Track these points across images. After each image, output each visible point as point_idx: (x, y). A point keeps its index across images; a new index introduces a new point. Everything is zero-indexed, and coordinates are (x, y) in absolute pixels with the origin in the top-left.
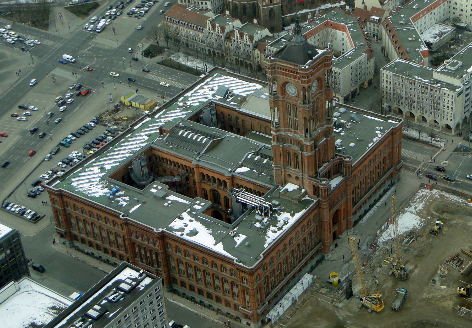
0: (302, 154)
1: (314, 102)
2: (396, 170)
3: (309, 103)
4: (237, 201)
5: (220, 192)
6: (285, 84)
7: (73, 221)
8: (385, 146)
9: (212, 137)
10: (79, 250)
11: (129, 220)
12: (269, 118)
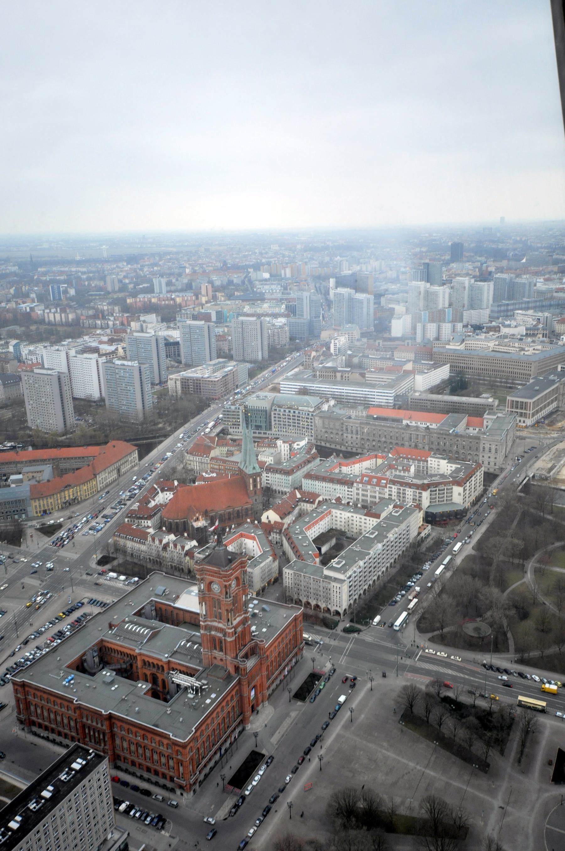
0: (225, 639)
1: (233, 597)
2: (299, 649)
4: (173, 682)
5: (158, 675)
6: (210, 583)
7: (32, 708)
8: (290, 630)
9: (152, 628)
10: (35, 734)
11: (81, 704)
12: (198, 611)
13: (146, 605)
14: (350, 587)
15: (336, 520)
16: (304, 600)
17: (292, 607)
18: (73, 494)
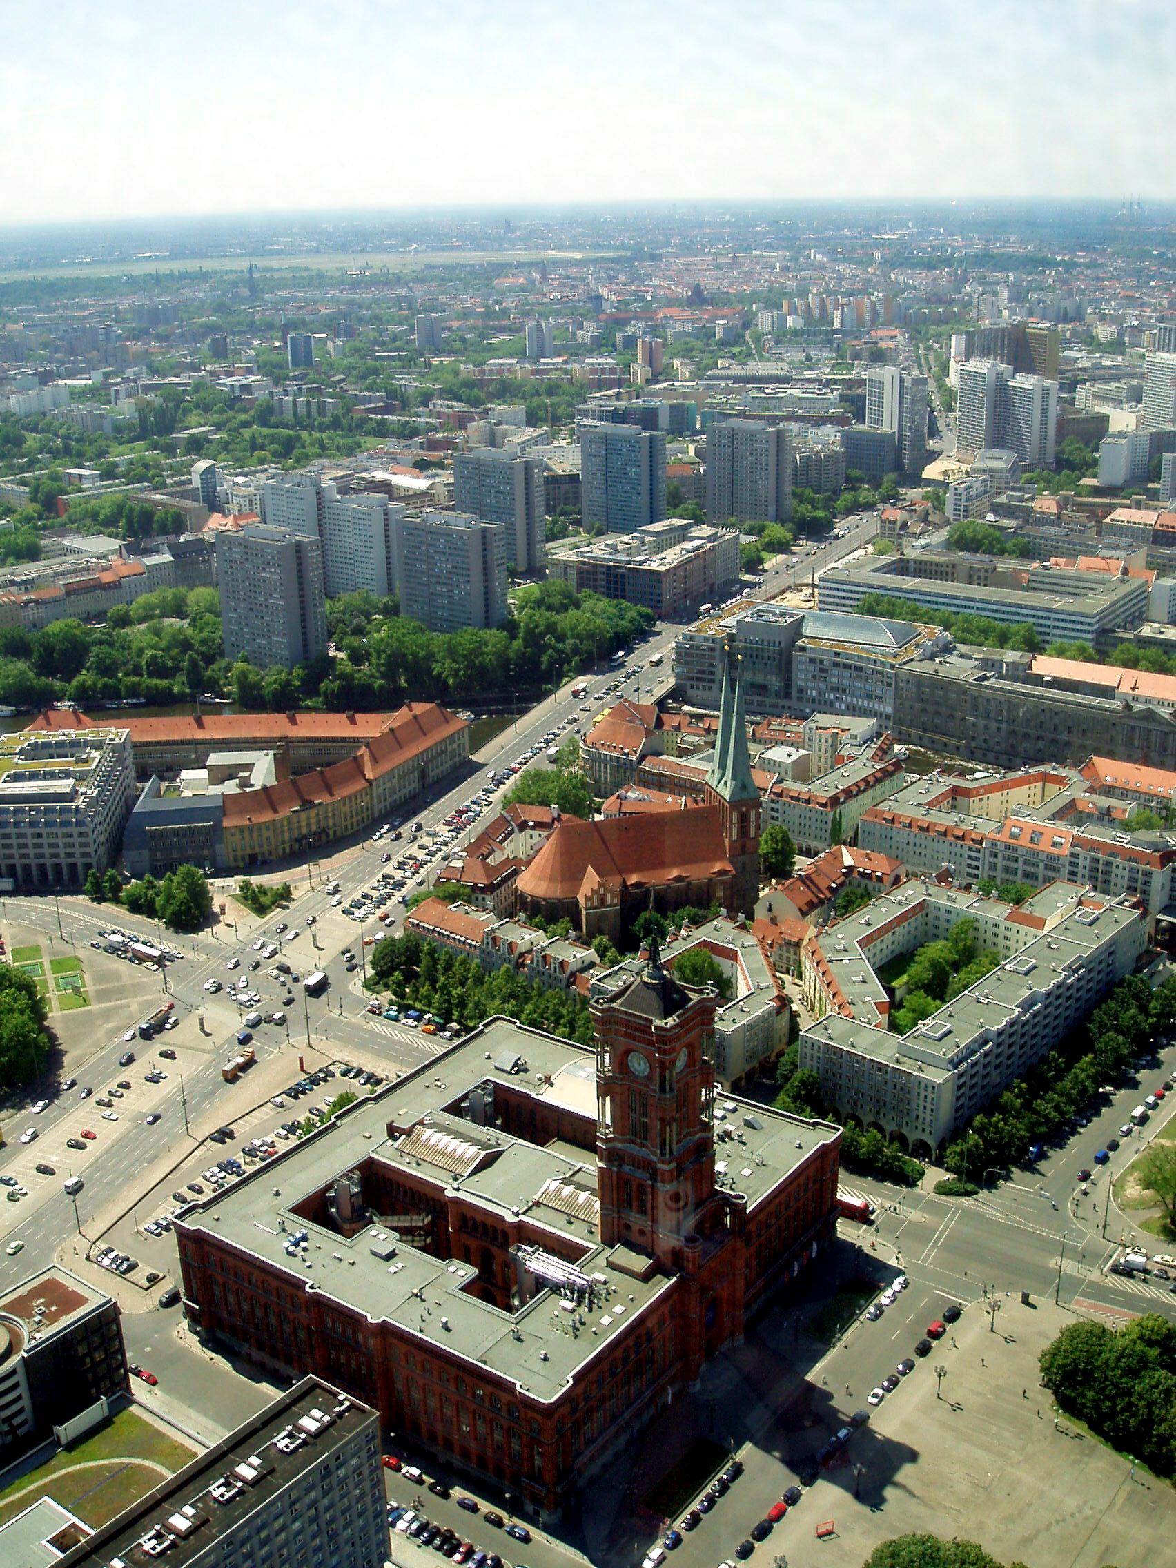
0: (653, 1187)
3: (671, 1089)
6: (627, 1052)
7: (217, 1291)
9: (484, 1146)
12: (593, 1115)
13: (472, 1091)
14: (959, 1087)
15: (936, 927)
16: (846, 1109)
17: (815, 1124)
18: (318, 821)
